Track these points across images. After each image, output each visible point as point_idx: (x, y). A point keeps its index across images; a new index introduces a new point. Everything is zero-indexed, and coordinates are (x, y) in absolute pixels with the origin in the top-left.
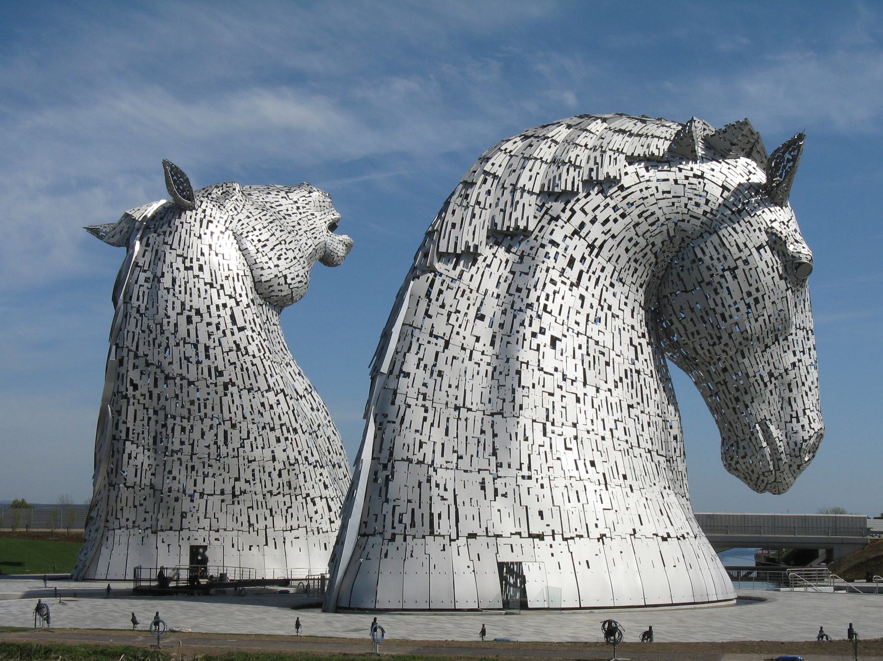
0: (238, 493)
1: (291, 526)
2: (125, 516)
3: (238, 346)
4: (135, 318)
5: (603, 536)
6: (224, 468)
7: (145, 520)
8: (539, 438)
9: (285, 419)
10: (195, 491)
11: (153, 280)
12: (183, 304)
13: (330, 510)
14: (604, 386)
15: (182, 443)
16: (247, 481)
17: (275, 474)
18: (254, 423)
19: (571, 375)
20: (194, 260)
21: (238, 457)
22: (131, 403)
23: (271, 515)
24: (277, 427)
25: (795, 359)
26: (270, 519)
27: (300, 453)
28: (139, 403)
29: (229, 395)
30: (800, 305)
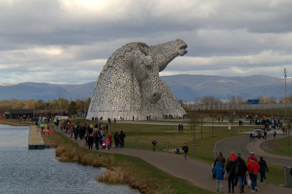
8: (105, 97)
14: (118, 89)
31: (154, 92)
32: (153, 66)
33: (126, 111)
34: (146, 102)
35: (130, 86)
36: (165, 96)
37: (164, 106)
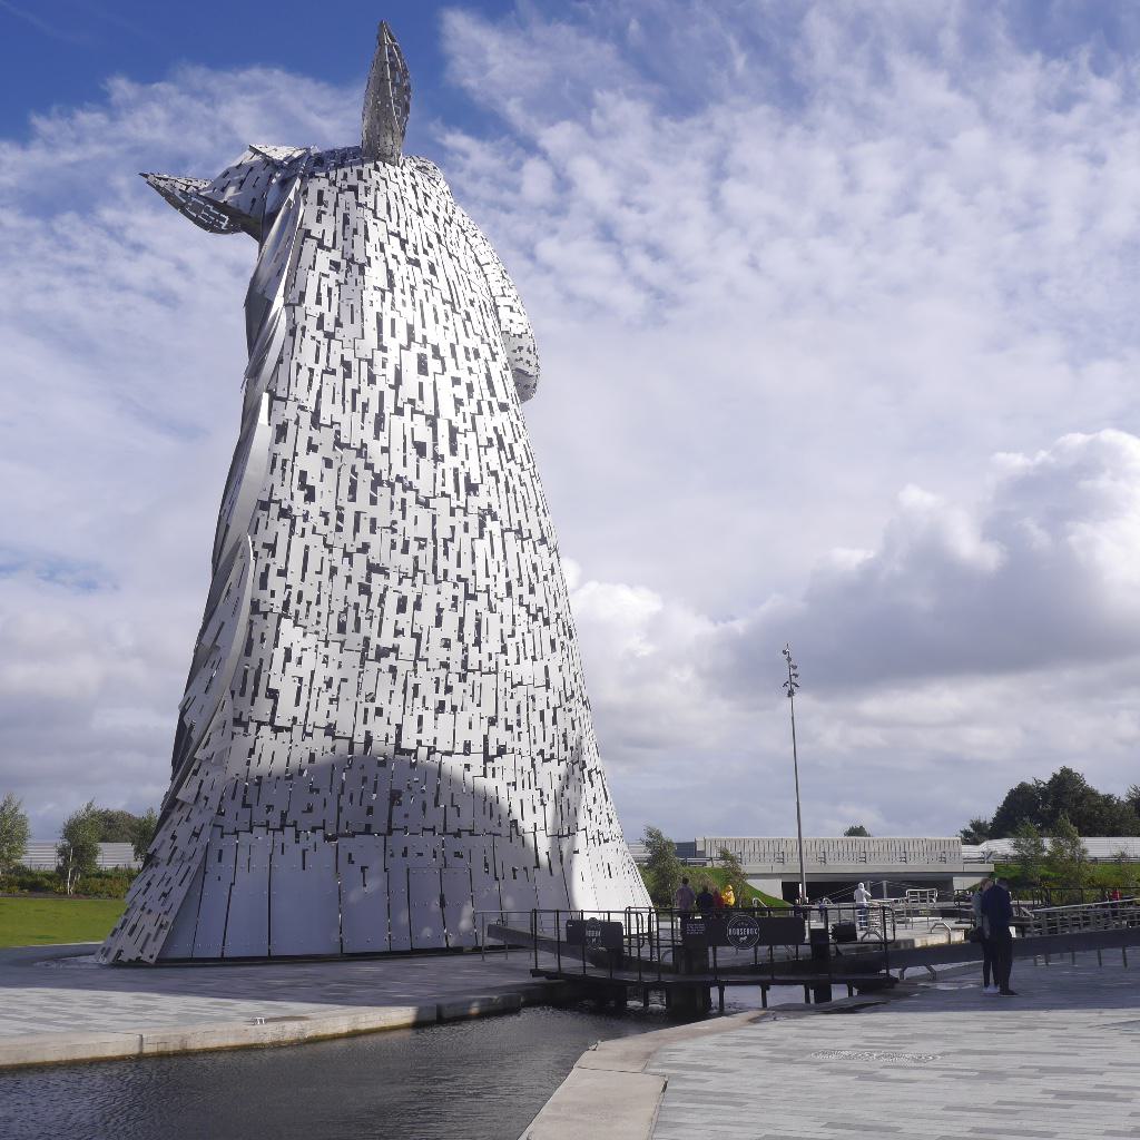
0: (492, 752)
2: (263, 804)
3: (500, 438)
4: (313, 338)
6: (472, 696)
7: (310, 810)
10: (419, 743)
11: (349, 269)
12: (410, 328)
15: (398, 633)
16: (509, 728)
17: (549, 715)
20: (420, 250)
21: (496, 673)
22: (298, 530)
23: (542, 803)
26: (540, 808)
28: (314, 532)
29: (487, 536)
34: (499, 735)
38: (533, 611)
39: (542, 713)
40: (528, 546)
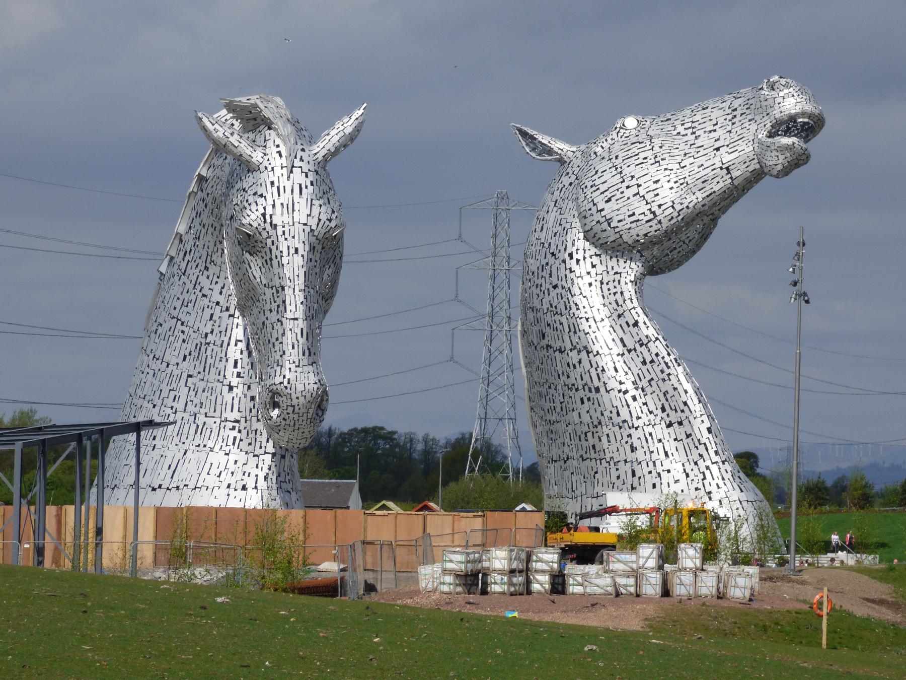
1: (597, 493)
5: (116, 486)
9: (586, 378)
13: (634, 474)
18: (565, 385)
19: (156, 356)
24: (581, 387)
25: (264, 319)
27: (602, 415)
30: (267, 264)
31: (269, 382)
32: (272, 232)
33: (178, 488)
35: (222, 346)
36: (652, 417)
37: (634, 474)
38: (570, 386)
39: (580, 436)
40: (564, 355)
